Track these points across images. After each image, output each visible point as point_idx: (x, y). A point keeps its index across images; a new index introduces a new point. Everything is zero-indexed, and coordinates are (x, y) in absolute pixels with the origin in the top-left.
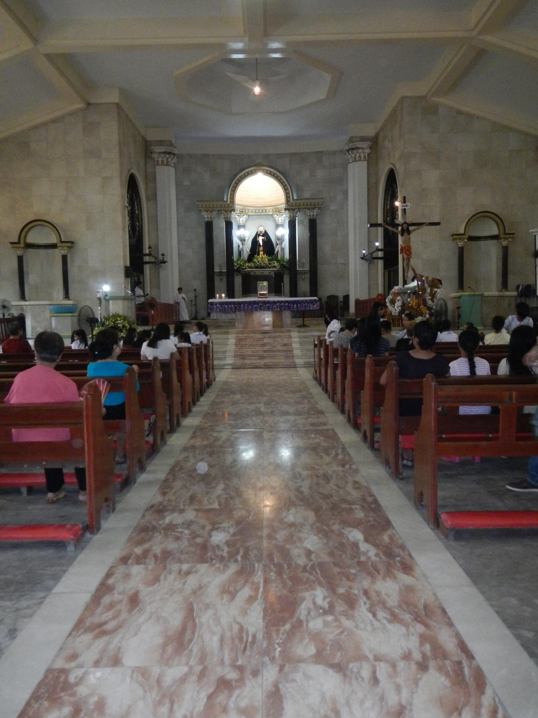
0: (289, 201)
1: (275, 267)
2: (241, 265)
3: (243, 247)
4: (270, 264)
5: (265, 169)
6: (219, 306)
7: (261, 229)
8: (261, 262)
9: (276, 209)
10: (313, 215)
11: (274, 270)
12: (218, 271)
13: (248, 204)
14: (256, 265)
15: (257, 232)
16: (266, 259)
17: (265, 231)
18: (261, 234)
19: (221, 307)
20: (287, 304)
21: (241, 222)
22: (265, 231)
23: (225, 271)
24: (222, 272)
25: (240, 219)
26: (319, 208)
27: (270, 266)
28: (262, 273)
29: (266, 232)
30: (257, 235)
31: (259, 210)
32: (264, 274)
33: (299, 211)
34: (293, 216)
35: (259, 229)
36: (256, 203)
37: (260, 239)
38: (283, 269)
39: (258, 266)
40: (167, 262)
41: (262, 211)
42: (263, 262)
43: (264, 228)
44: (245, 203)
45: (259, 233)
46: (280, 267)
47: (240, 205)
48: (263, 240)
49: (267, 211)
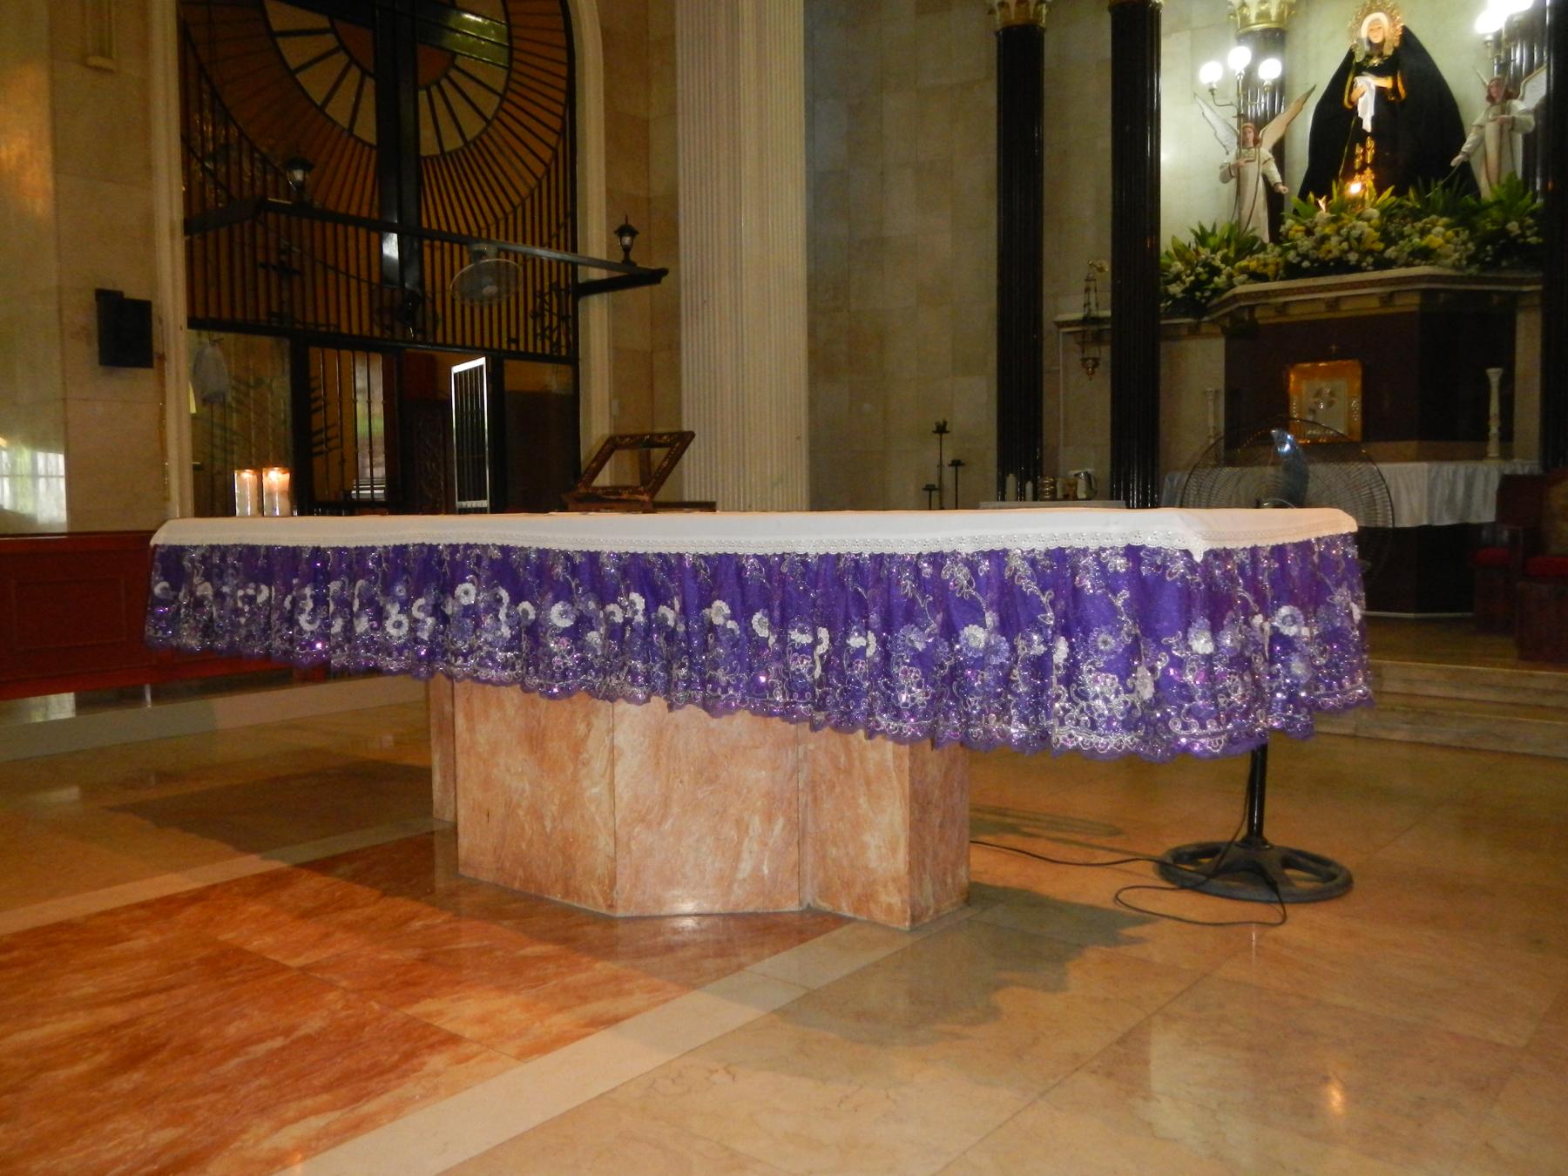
1: (1426, 254)
2: (1216, 271)
3: (1239, 156)
4: (1388, 239)
6: (205, 589)
7: (1375, 26)
8: (1328, 230)
11: (1419, 279)
12: (1079, 315)
14: (1291, 255)
15: (1351, 55)
16: (1375, 213)
17: (1407, 37)
18: (1375, 61)
19: (219, 595)
20: (719, 612)
21: (1252, 14)
22: (1407, 37)
23: (1108, 313)
24: (1098, 321)
27: (1391, 252)
28: (1334, 304)
29: (1408, 39)
30: (1350, 68)
32: (1347, 309)
35: (1364, 33)
37: (1365, 93)
38: (1486, 266)
39: (1304, 257)
40: (664, 272)
42: (1338, 233)
43: (1392, 18)
45: (1359, 58)
46: (1472, 259)
48: (1380, 92)
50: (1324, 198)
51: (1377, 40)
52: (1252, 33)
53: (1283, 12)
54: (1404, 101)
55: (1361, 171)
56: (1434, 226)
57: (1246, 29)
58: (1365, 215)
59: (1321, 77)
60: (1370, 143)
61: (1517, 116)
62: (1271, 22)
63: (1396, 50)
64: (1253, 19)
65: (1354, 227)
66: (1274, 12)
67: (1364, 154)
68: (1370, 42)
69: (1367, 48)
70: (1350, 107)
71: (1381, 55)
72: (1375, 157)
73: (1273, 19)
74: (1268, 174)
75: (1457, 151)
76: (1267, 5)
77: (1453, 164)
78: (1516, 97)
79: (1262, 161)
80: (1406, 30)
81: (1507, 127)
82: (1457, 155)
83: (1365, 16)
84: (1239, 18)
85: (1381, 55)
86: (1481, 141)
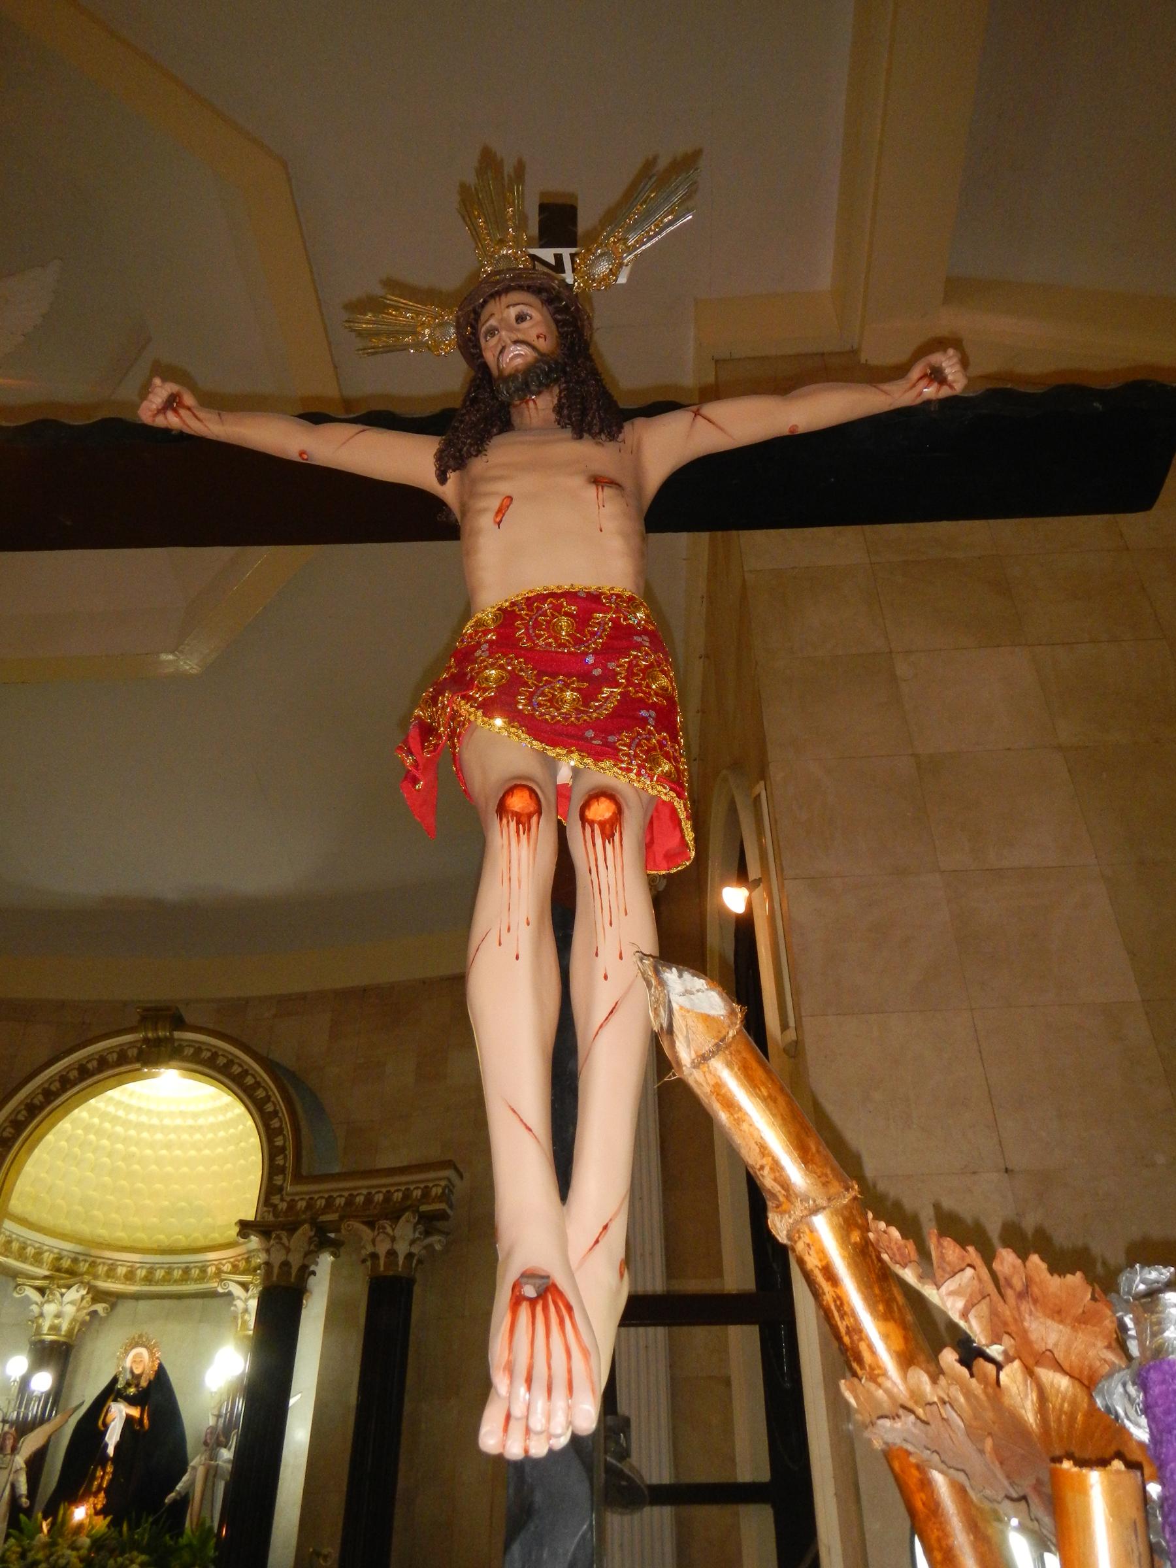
0: (280, 1189)
5: (191, 1043)
8: (40, 1556)
9: (248, 1260)
10: (392, 1253)
13: (121, 1235)
15: (115, 1380)
16: (85, 1541)
18: (132, 1391)
22: (161, 1375)
25: (50, 1309)
26: (430, 1222)
31: (169, 1271)
33: (323, 1241)
34: (286, 1264)
35: (128, 1363)
36: (161, 1237)
41: (187, 1271)
42: (47, 1558)
43: (151, 1354)
44: (103, 1232)
47: (63, 1236)
48: (129, 1420)
49: (211, 1270)
50: (49, 1520)
51: (137, 1372)
52: (42, 1342)
53: (73, 1329)
54: (148, 1430)
55: (96, 1494)
56: (132, 1562)
57: (38, 1338)
58: (79, 1544)
59: (87, 1391)
60: (110, 1469)
61: (220, 1463)
62: (60, 1335)
63: (150, 1383)
64: (45, 1330)
65: (63, 1556)
66: (65, 1327)
67: (103, 1477)
68: (132, 1372)
69: (129, 1376)
70: (102, 1429)
71: (137, 1386)
72: (111, 1482)
73: (63, 1333)
74: (17, 1485)
75: (172, 1489)
76: (60, 1320)
77: (166, 1501)
78: (225, 1447)
79: (13, 1470)
80: (161, 1366)
81: (212, 1472)
82: (171, 1491)
83: (133, 1348)
84: (35, 1325)
85: (137, 1386)
86: (192, 1483)
